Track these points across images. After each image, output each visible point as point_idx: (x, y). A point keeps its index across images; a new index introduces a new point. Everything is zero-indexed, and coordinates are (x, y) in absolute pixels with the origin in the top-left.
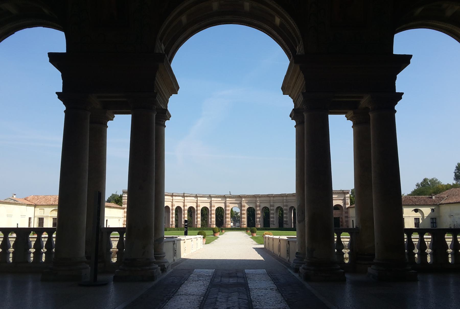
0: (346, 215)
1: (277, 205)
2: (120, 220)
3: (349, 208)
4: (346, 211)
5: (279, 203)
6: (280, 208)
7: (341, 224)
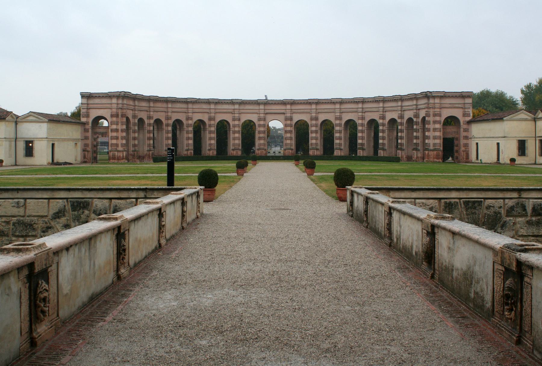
0: (465, 134)
1: (346, 117)
2: (78, 144)
3: (469, 122)
5: (350, 114)
7: (455, 148)
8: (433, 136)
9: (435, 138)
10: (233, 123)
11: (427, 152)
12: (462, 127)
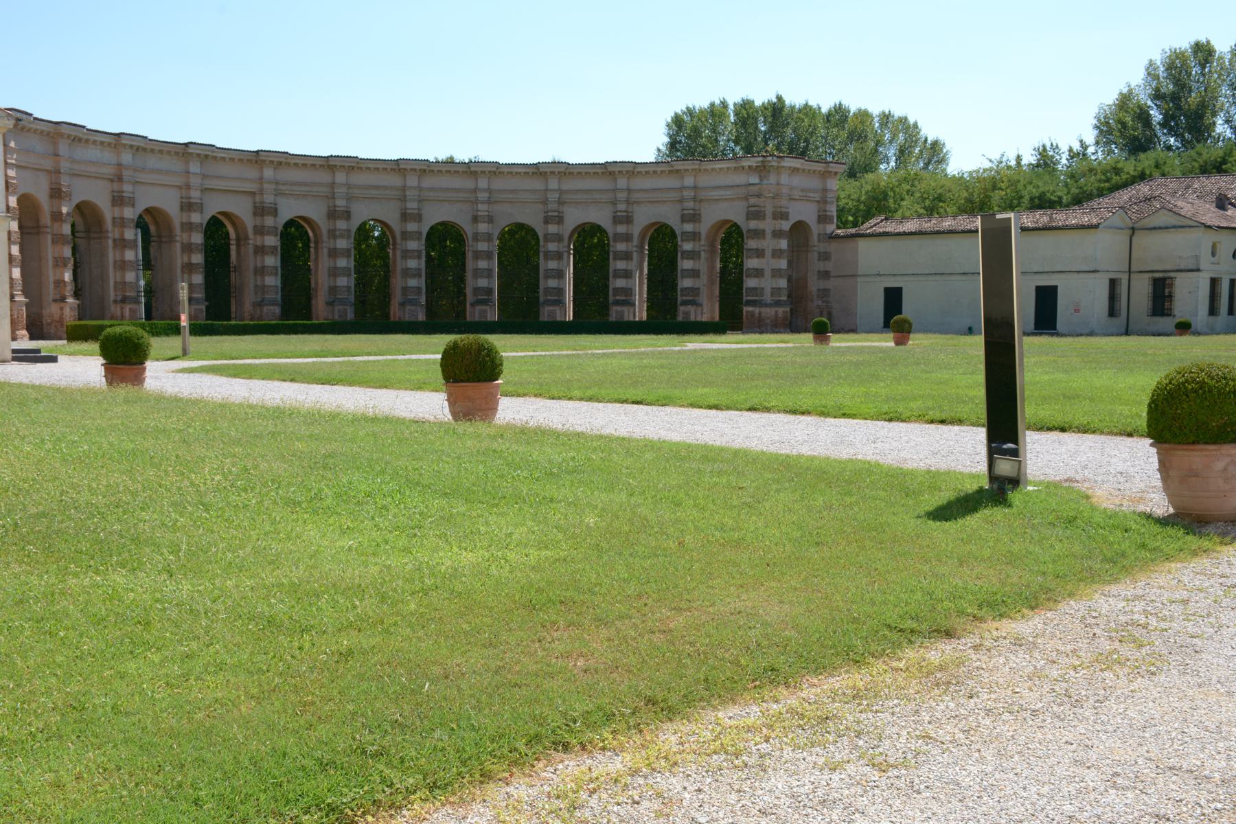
0: (822, 266)
4: (822, 250)
6: (664, 228)
8: (773, 270)
9: (776, 273)
10: (117, 212)
11: (757, 310)
12: (816, 249)
